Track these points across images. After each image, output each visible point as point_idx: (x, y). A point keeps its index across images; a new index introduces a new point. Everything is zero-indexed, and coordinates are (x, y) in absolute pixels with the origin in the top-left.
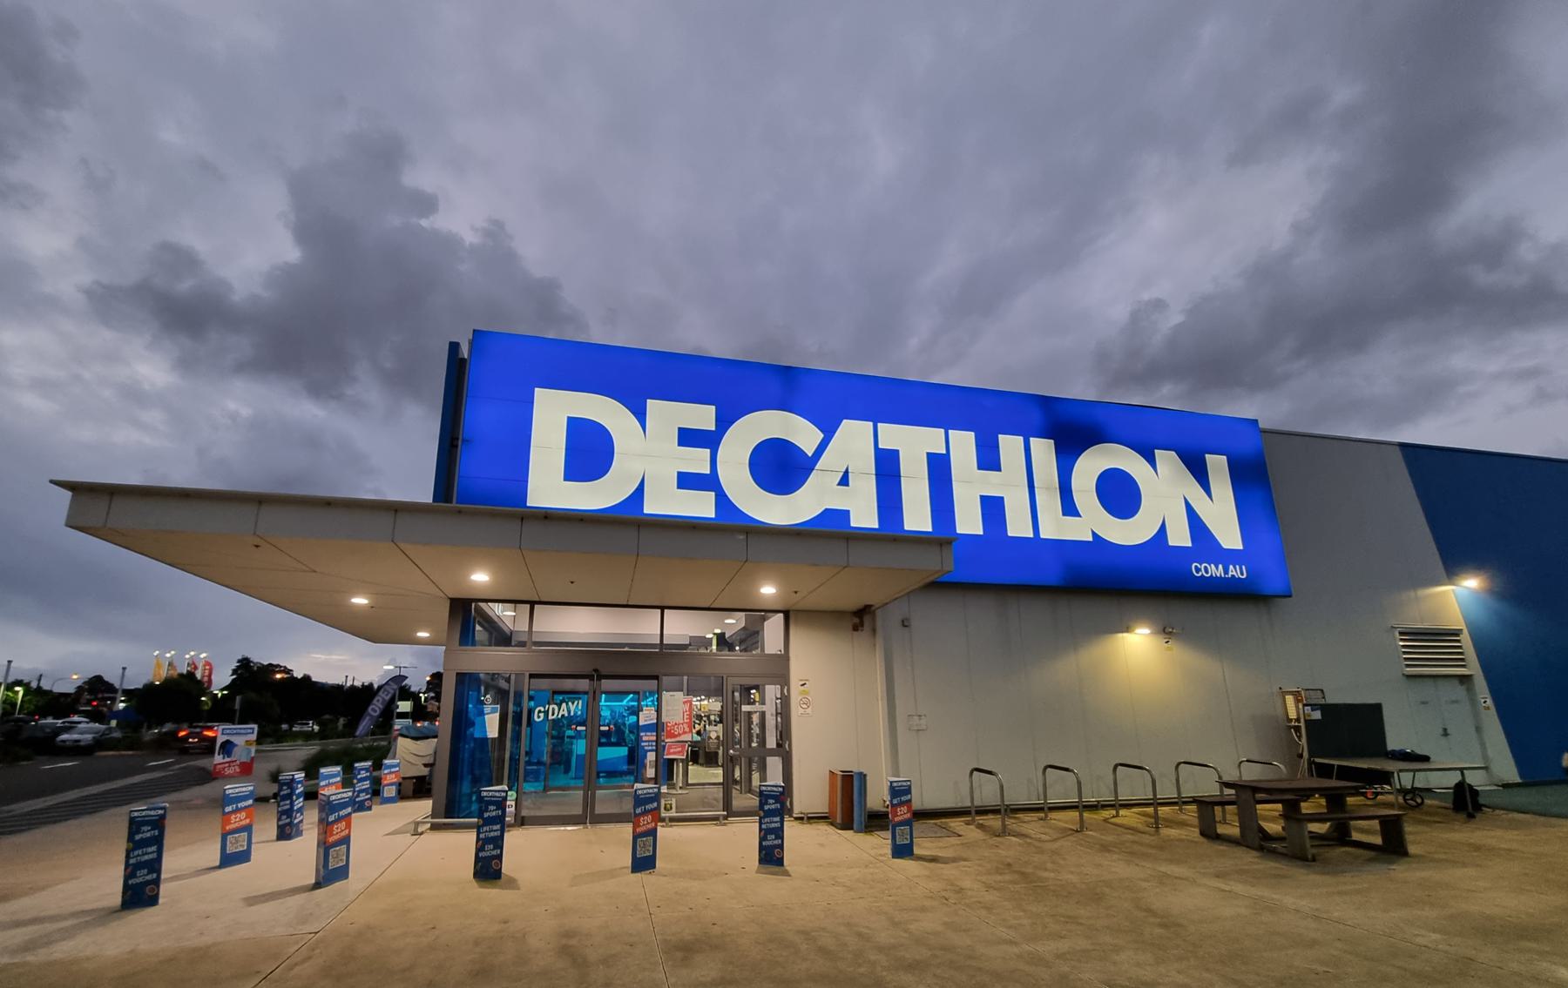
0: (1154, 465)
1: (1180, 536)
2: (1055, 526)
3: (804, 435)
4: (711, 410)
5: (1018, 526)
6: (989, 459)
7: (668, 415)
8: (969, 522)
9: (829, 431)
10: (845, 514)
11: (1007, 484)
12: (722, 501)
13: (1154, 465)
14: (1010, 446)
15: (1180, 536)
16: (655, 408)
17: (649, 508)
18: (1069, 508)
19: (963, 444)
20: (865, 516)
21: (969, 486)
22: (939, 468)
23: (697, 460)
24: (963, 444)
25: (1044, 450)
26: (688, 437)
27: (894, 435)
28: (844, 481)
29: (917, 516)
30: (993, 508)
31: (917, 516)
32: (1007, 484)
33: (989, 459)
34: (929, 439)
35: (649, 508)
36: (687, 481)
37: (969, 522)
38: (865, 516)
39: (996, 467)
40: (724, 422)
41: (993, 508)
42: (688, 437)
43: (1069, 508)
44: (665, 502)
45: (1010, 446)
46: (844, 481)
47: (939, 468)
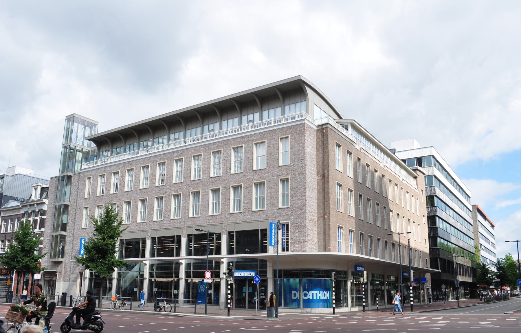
3: (307, 292)
6: (320, 293)
8: (318, 298)
9: (309, 292)
10: (309, 298)
14: (321, 292)
21: (319, 295)
22: (316, 294)
24: (318, 292)
28: (310, 296)
31: (315, 298)
37: (318, 298)
38: (311, 298)
47: (316, 294)
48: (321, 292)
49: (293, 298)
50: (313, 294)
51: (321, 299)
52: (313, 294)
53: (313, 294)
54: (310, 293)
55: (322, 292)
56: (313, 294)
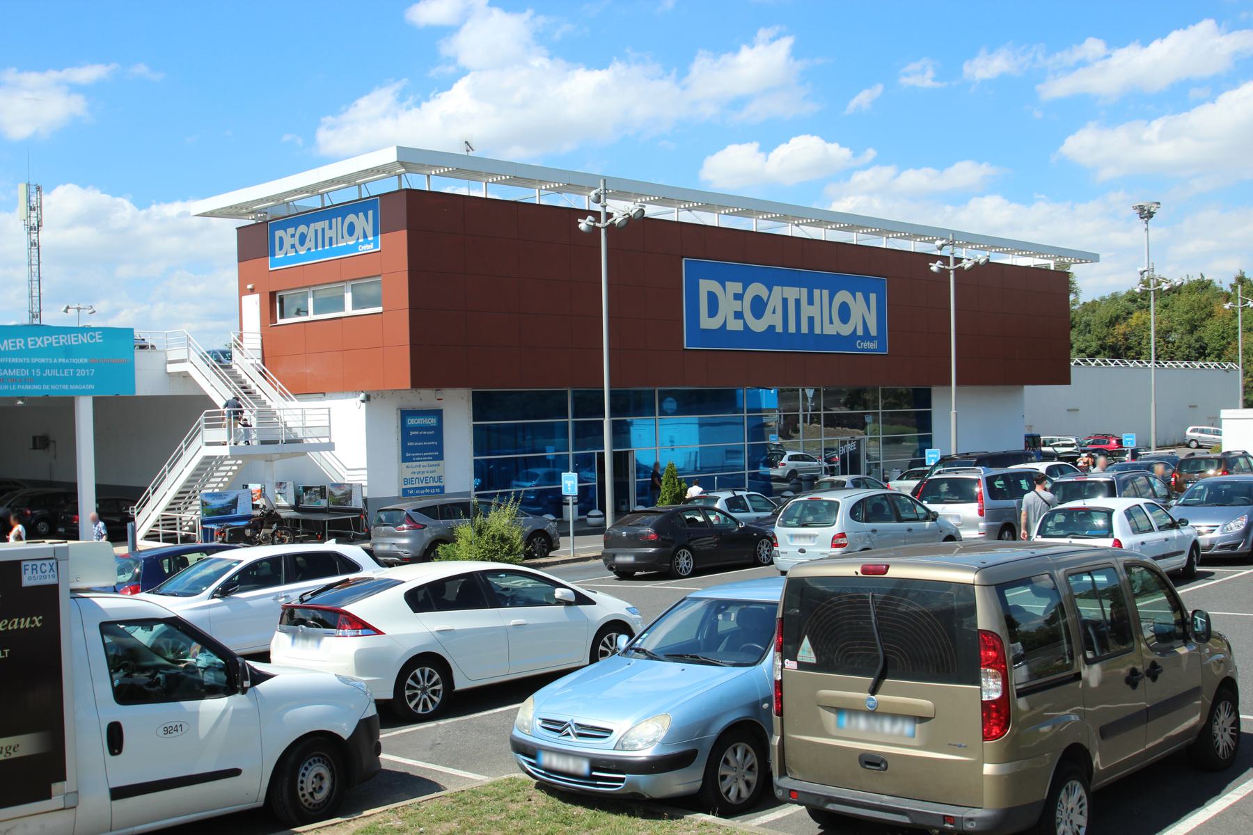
0: (855, 297)
1: (860, 332)
2: (830, 330)
4: (740, 285)
5: (817, 331)
6: (811, 302)
8: (805, 330)
12: (745, 324)
13: (855, 297)
14: (817, 292)
16: (728, 284)
17: (729, 328)
18: (831, 322)
20: (779, 329)
21: (807, 311)
22: (798, 302)
23: (737, 306)
25: (826, 293)
26: (738, 297)
28: (774, 312)
29: (792, 329)
31: (792, 329)
33: (811, 302)
35: (729, 328)
36: (739, 315)
38: (779, 329)
39: (813, 304)
40: (745, 289)
41: (811, 319)
42: (738, 297)
43: (831, 322)
44: (735, 325)
45: (817, 292)
46: (774, 312)
47: (798, 302)
48: (821, 295)
50: (787, 299)
51: (817, 331)
52: (785, 301)
53: (785, 301)
55: (826, 293)
56: (787, 299)
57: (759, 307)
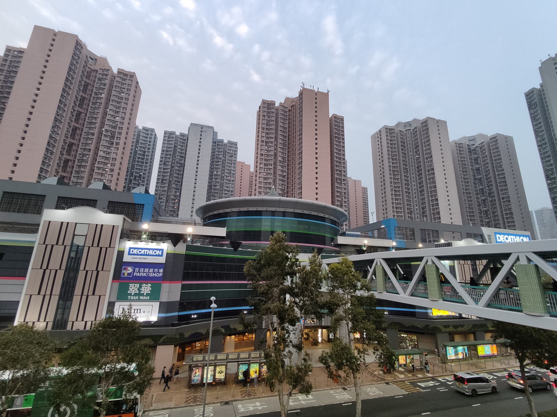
1: (158, 254)
2: (152, 254)
6: (149, 251)
7: (136, 250)
8: (148, 254)
11: (150, 252)
14: (150, 251)
15: (158, 254)
19: (148, 250)
22: (147, 252)
24: (148, 250)
25: (152, 251)
27: (145, 250)
29: (145, 253)
30: (149, 253)
31: (145, 253)
32: (150, 252)
33: (149, 251)
34: (147, 250)
37: (148, 254)
41: (149, 253)
44: (135, 253)
45: (150, 251)
47: (147, 252)
49: (131, 253)
52: (144, 251)
53: (144, 251)
54: (143, 250)
57: (140, 252)
